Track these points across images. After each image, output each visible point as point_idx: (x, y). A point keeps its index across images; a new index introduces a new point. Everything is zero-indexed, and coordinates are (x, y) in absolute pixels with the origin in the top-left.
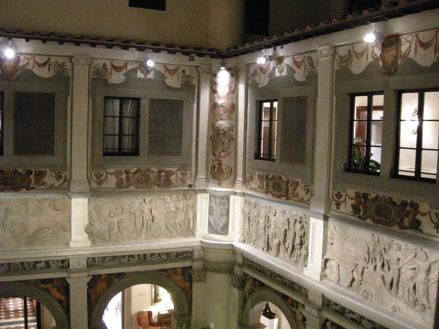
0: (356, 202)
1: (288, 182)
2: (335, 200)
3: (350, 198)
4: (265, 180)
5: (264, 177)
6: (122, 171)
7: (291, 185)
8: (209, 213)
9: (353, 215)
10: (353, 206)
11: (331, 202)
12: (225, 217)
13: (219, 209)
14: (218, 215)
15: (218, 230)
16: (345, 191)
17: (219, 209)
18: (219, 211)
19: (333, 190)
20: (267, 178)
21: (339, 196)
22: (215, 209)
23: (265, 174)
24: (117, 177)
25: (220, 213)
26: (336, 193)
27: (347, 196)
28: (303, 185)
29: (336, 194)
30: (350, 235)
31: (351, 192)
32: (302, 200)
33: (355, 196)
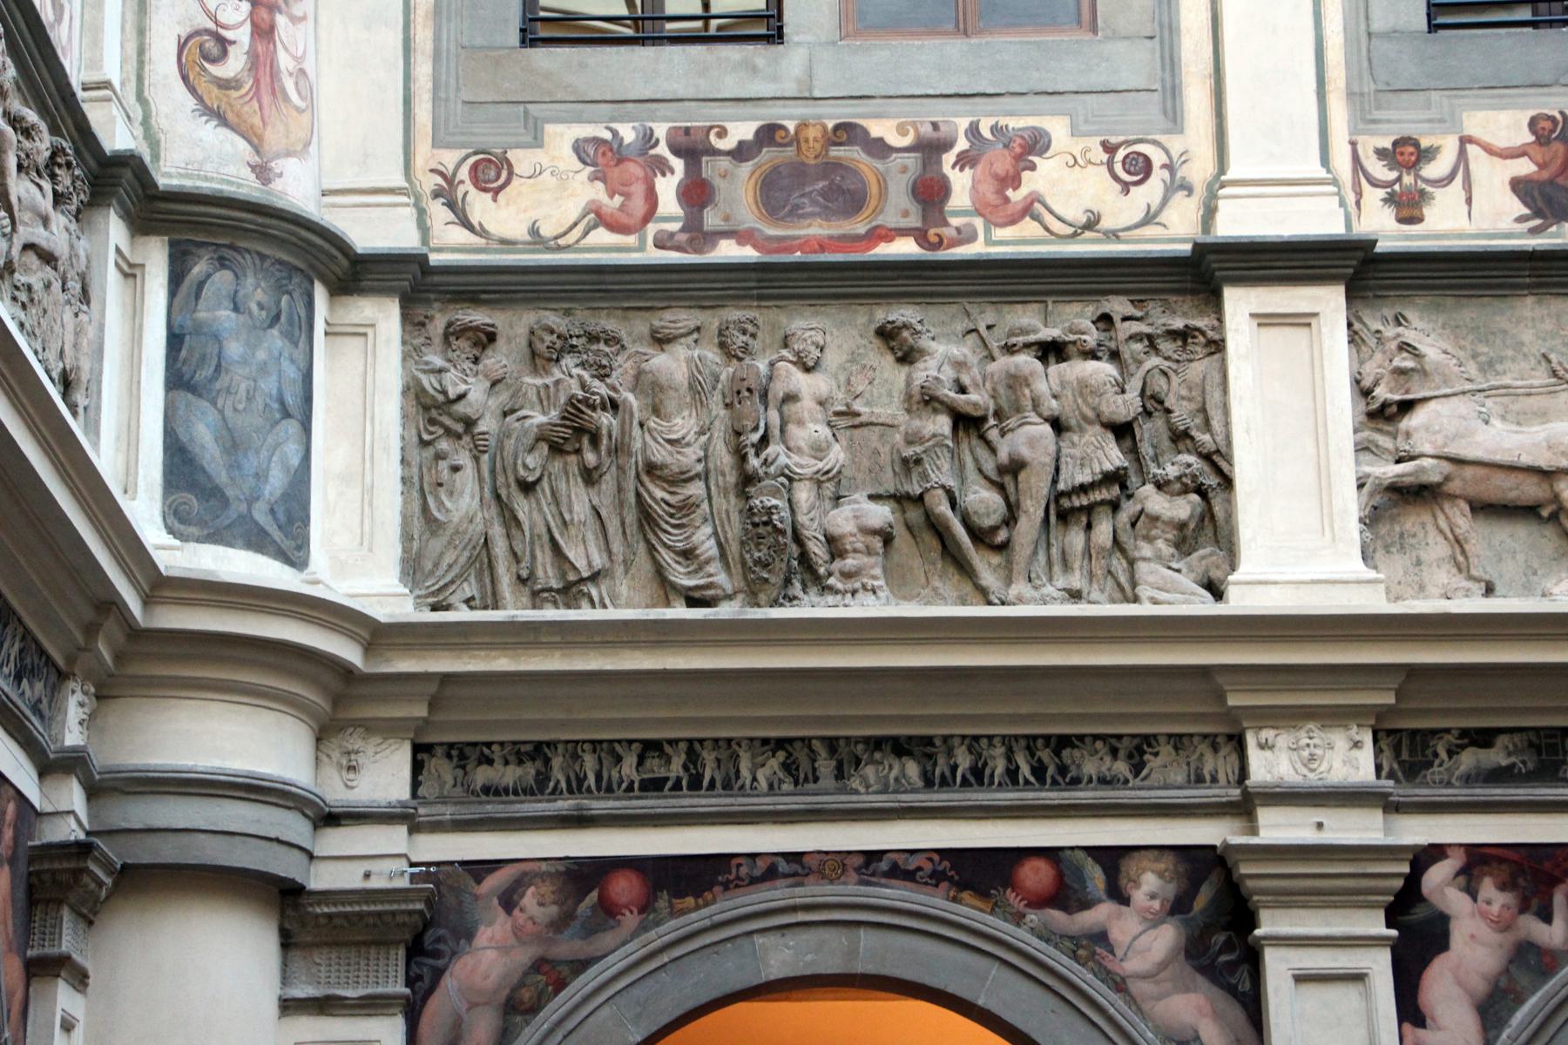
0: (1542, 166)
1: (931, 148)
2: (1374, 183)
3: (1490, 150)
4: (663, 167)
5: (663, 150)
7: (963, 161)
8: (178, 380)
9: (1534, 231)
10: (1519, 186)
11: (1351, 198)
12: (292, 427)
13: (261, 355)
14: (259, 402)
15: (260, 515)
17: (261, 355)
18: (263, 369)
19: (1354, 131)
20: (692, 149)
21: (1407, 154)
22: (234, 349)
23: (661, 130)
25: (269, 385)
26: (1387, 143)
27: (1472, 149)
28: (1094, 143)
29: (1381, 153)
30: (1527, 336)
31: (1506, 124)
32: (1091, 225)
33: (1532, 138)
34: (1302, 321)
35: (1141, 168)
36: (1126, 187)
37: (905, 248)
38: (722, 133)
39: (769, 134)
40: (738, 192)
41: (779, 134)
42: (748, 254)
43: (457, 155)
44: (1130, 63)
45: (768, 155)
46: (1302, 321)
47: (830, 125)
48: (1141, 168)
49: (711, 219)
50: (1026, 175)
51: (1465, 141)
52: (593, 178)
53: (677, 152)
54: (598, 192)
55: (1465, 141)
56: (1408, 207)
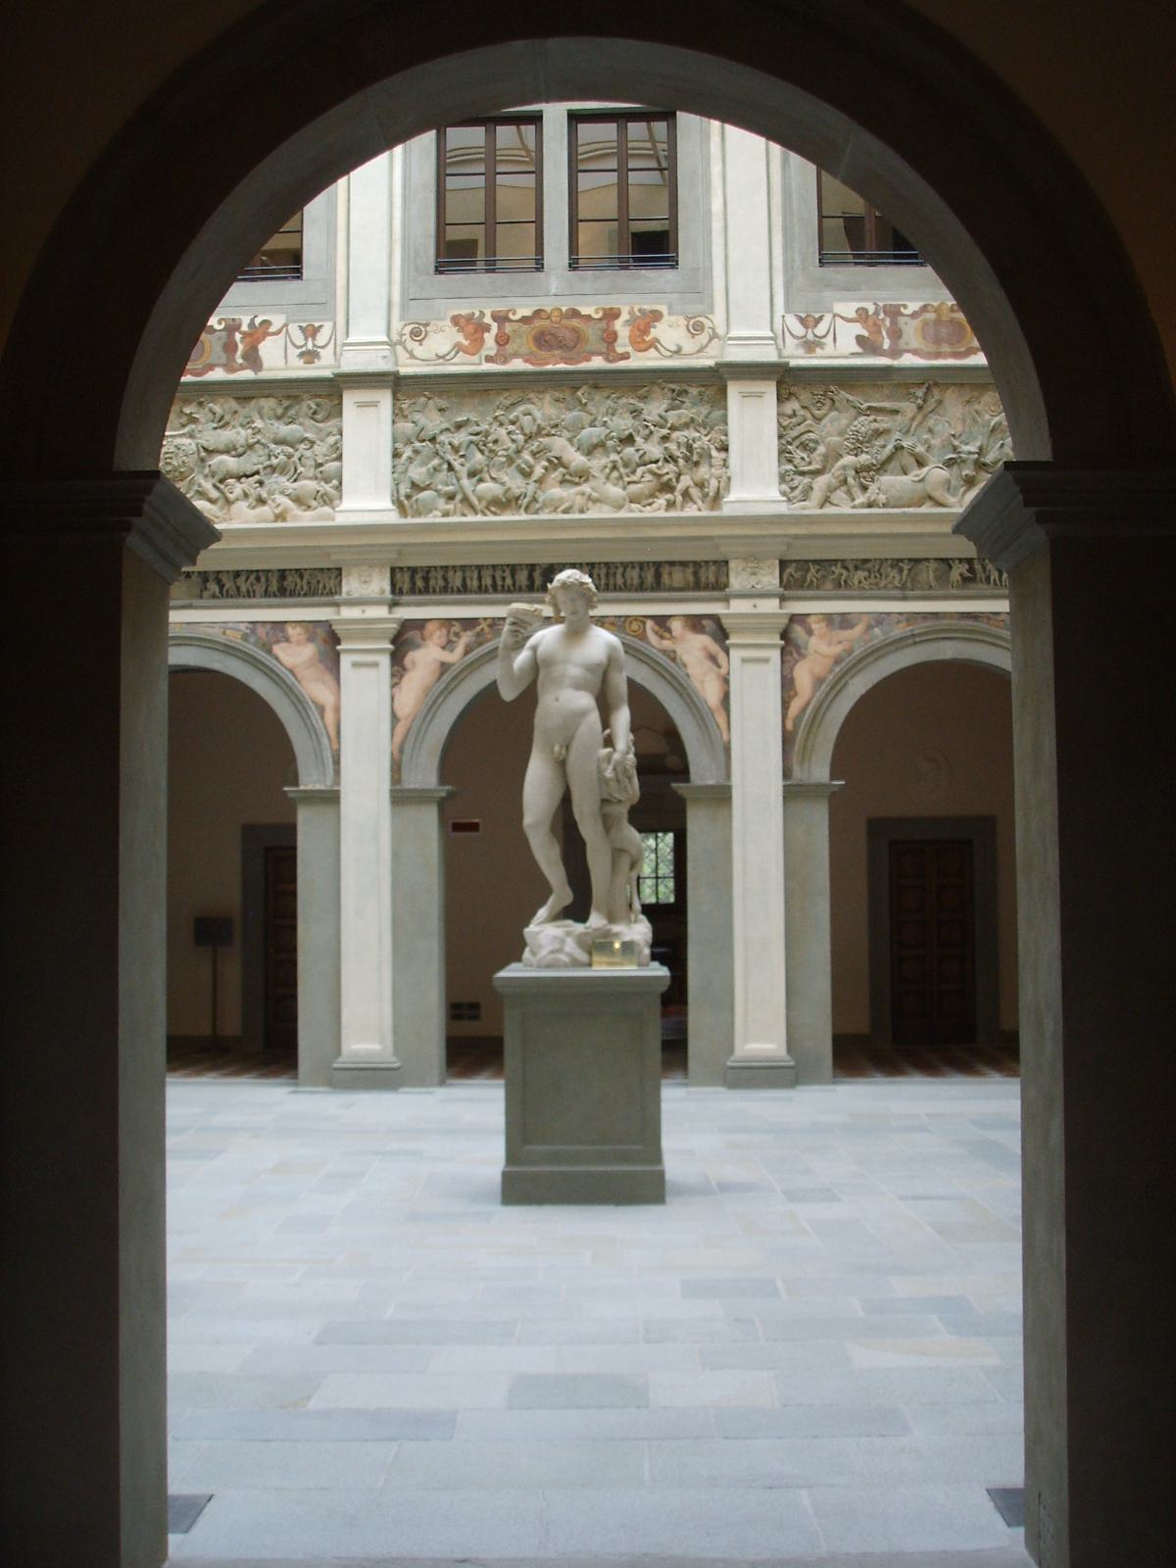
20: (501, 318)
34: (760, 395)
35: (699, 328)
36: (693, 335)
37: (597, 363)
39: (538, 313)
40: (523, 342)
41: (542, 314)
42: (529, 367)
45: (538, 323)
47: (564, 309)
48: (699, 328)
49: (510, 348)
50: (652, 330)
51: (834, 316)
52: (458, 331)
53: (495, 318)
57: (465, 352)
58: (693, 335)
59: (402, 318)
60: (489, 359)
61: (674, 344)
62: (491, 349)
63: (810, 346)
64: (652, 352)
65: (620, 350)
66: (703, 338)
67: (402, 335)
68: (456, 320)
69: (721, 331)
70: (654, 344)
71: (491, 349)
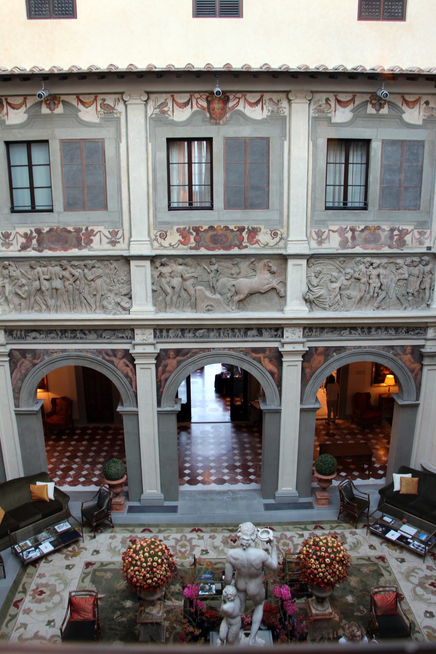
6: (346, 228)
16: (327, 227)
24: (340, 236)
35: (276, 234)
38: (202, 228)
43: (156, 231)
44: (275, 216)
46: (300, 265)
48: (276, 234)
51: (329, 230)
54: (180, 238)
55: (329, 230)
56: (320, 243)
57: (182, 244)
58: (273, 238)
59: (154, 229)
60: (191, 248)
61: (265, 242)
62: (193, 243)
63: (320, 243)
64: (256, 246)
65: (244, 244)
66: (278, 239)
67: (156, 236)
68: (178, 230)
69: (284, 236)
70: (257, 242)
71: (193, 243)
